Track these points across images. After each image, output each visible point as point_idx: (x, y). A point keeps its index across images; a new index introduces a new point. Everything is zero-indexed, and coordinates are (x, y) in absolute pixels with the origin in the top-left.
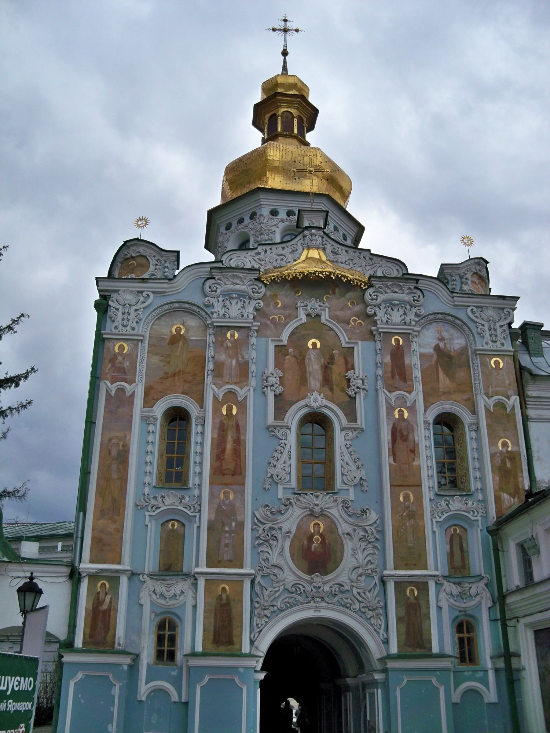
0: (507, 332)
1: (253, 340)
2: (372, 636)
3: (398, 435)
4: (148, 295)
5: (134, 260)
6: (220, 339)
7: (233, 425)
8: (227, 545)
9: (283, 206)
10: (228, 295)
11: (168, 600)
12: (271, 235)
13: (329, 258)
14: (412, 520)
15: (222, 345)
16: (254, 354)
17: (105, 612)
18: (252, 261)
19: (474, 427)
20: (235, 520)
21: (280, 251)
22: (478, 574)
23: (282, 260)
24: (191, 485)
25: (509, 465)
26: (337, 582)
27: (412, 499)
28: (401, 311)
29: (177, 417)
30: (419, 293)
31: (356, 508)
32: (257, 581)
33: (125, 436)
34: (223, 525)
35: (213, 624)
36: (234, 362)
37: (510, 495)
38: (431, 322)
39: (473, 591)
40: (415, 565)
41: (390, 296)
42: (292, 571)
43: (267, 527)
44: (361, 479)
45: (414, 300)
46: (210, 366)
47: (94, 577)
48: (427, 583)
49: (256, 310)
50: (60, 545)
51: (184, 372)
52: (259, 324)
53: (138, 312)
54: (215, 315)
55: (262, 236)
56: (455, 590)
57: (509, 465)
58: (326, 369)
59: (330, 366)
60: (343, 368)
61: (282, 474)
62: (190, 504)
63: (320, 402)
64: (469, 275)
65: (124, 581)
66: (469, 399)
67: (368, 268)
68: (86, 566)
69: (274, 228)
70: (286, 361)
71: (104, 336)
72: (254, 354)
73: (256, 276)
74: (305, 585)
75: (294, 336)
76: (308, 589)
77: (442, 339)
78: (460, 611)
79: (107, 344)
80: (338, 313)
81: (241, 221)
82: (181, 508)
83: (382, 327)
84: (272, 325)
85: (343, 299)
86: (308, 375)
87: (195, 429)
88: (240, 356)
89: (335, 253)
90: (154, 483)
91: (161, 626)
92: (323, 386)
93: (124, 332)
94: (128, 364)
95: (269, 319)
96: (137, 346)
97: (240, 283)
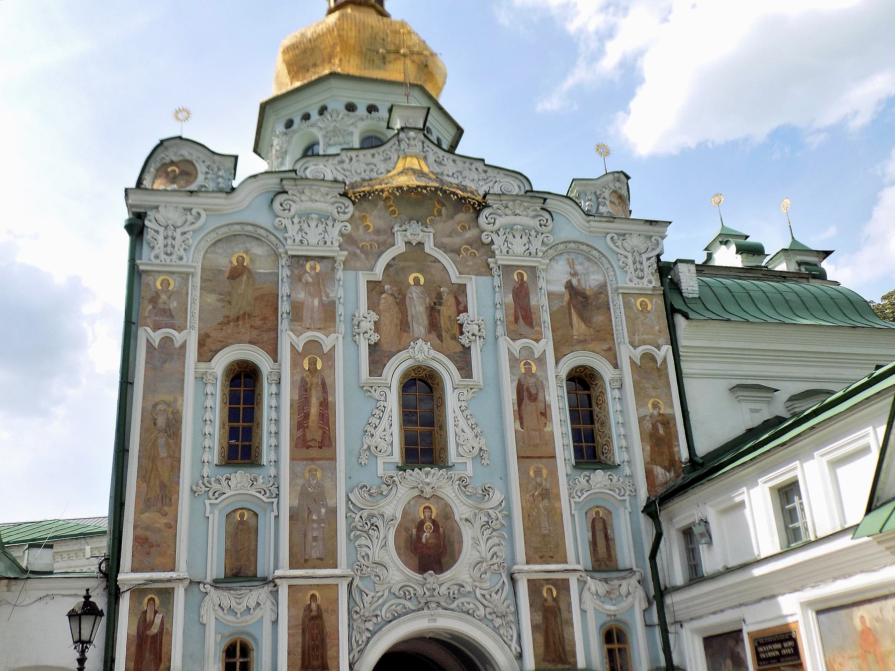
0: (655, 266)
1: (340, 274)
2: (503, 651)
3: (525, 394)
4: (199, 214)
5: (174, 164)
6: (296, 272)
7: (317, 384)
8: (315, 539)
9: (362, 97)
10: (305, 216)
11: (239, 615)
12: (349, 138)
13: (431, 169)
14: (546, 501)
15: (300, 280)
16: (341, 293)
17: (155, 637)
18: (335, 172)
19: (617, 385)
20: (325, 506)
21: (370, 159)
22: (629, 567)
23: (372, 170)
24: (264, 461)
25: (661, 431)
26: (456, 582)
27: (545, 472)
28: (525, 239)
30: (547, 216)
31: (477, 485)
32: (355, 584)
33: (176, 401)
34: (310, 512)
35: (300, 645)
36: (316, 302)
37: (665, 468)
38: (561, 254)
39: (623, 590)
40: (552, 557)
41: (512, 219)
42: (399, 569)
43: (365, 514)
44: (481, 449)
45: (541, 225)
46: (284, 307)
47: (138, 592)
48: (567, 581)
49: (341, 234)
50: (88, 548)
51: (250, 316)
52: (346, 253)
53: (187, 236)
54: (290, 241)
55: (337, 138)
56: (602, 588)
57: (661, 431)
58: (433, 311)
59: (438, 307)
60: (454, 309)
61: (383, 445)
62: (264, 487)
63: (426, 354)
64: (607, 194)
66: (610, 349)
67: (481, 183)
68: (126, 576)
69: (351, 129)
70: (383, 301)
71: (141, 268)
72: (341, 293)
74: (416, 587)
75: (391, 269)
76: (420, 591)
77: (575, 274)
78: (608, 615)
80: (446, 240)
81: (306, 117)
84: (363, 256)
85: (451, 222)
86: (410, 319)
87: (267, 389)
88: (323, 294)
89: (440, 163)
90: (216, 461)
91: (230, 652)
92: (430, 332)
93: (168, 263)
94: (175, 305)
95: (358, 247)
96: (187, 280)
97: (322, 199)
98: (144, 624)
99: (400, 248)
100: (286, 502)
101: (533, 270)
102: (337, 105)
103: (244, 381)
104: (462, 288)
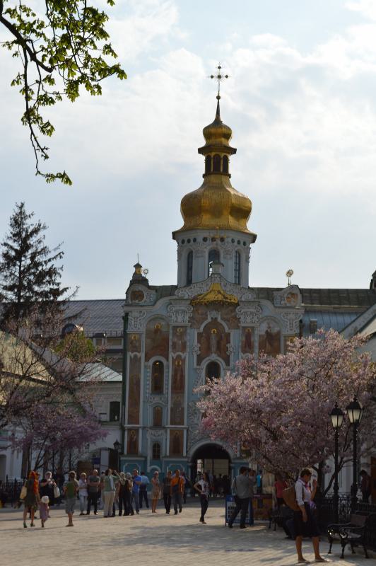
1: (188, 331)
10: (177, 312)
21: (201, 286)
29: (158, 368)
46: (170, 343)
47: (129, 430)
49: (189, 317)
58: (219, 343)
64: (285, 295)
65: (141, 431)
68: (127, 426)
69: (205, 250)
73: (189, 302)
77: (269, 328)
79: (129, 336)
81: (189, 241)
82: (161, 402)
83: (242, 325)
87: (165, 370)
101: (253, 328)
102: (200, 239)
104: (229, 334)
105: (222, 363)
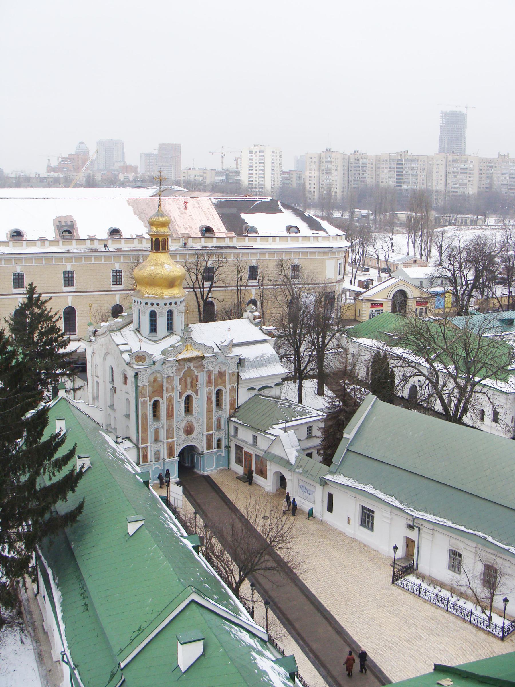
10: (168, 367)
46: (164, 388)
47: (142, 448)
58: (191, 382)
68: (141, 446)
98: (144, 453)
99: (186, 368)
100: (165, 427)
103: (156, 404)
105: (194, 396)
